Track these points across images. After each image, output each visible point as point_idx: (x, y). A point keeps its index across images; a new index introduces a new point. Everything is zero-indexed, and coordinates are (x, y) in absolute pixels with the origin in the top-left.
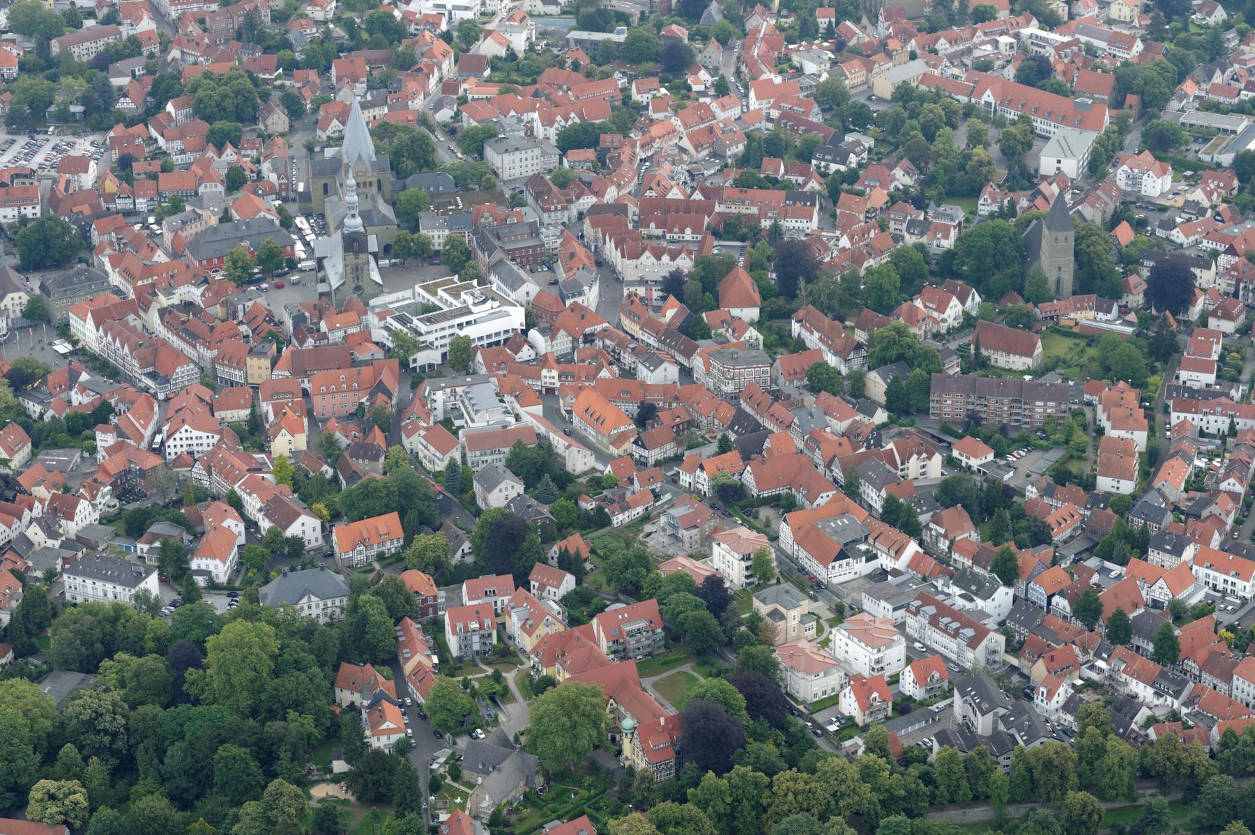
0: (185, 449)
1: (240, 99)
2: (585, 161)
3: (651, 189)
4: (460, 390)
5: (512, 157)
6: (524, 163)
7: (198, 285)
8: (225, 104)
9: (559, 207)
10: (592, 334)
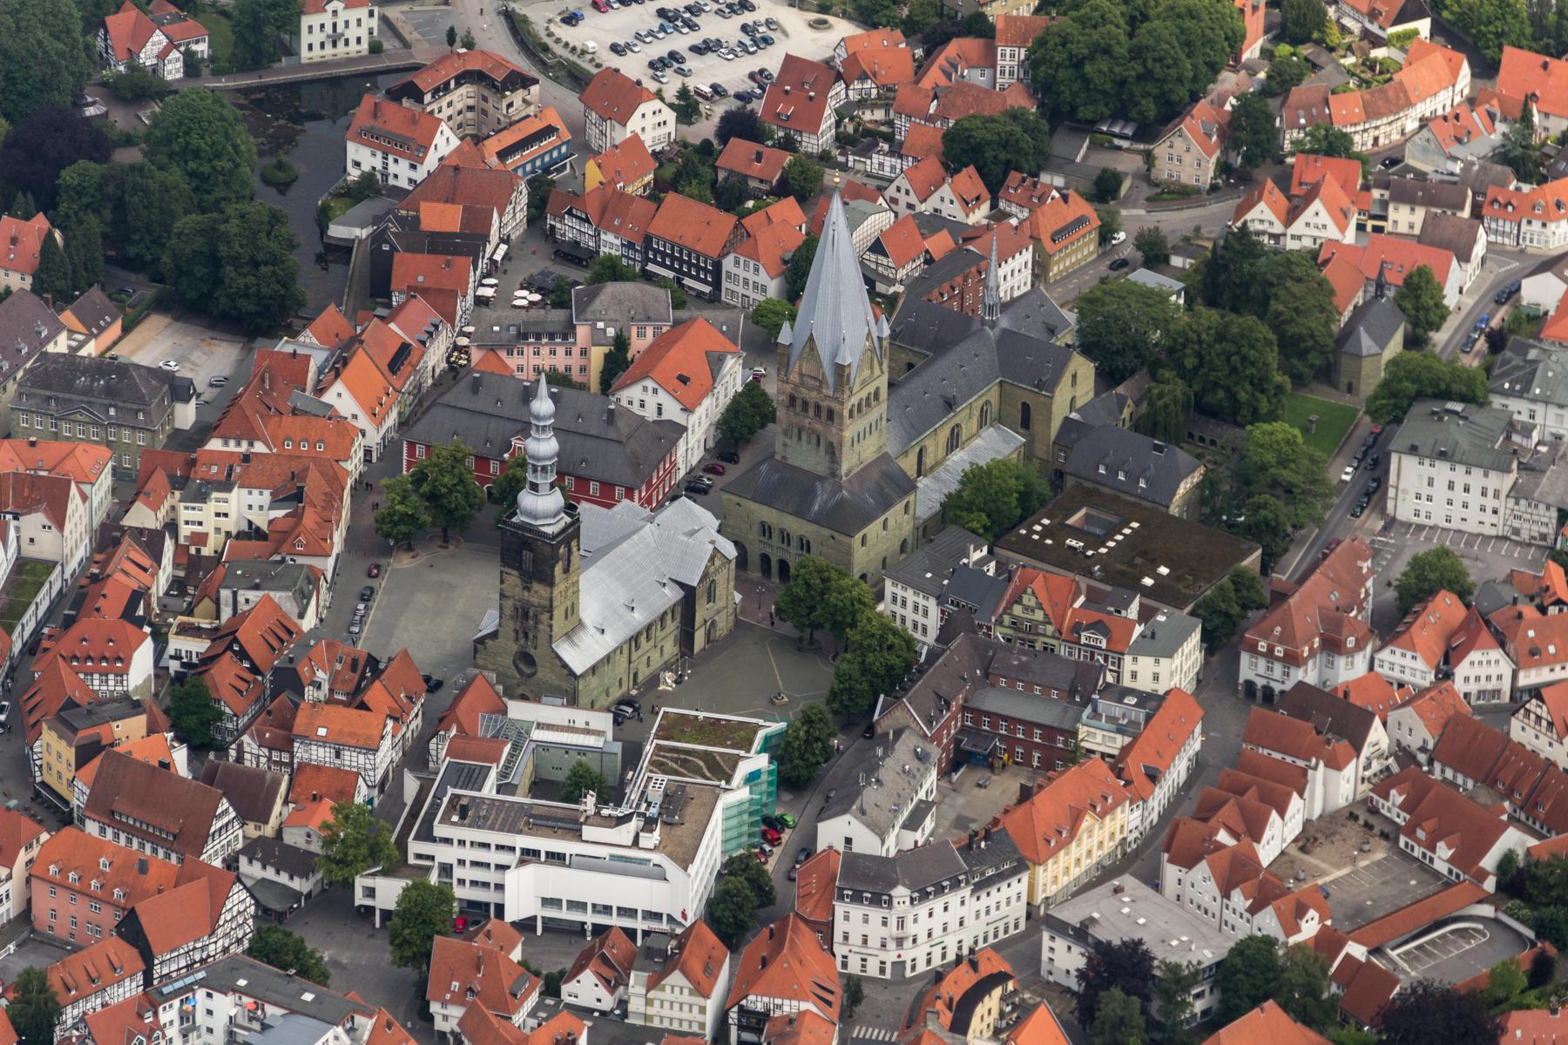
3: (1539, 697)
4: (270, 1009)
5: (1426, 470)
6: (1458, 495)
7: (276, 502)
9: (1279, 651)
10: (764, 1016)
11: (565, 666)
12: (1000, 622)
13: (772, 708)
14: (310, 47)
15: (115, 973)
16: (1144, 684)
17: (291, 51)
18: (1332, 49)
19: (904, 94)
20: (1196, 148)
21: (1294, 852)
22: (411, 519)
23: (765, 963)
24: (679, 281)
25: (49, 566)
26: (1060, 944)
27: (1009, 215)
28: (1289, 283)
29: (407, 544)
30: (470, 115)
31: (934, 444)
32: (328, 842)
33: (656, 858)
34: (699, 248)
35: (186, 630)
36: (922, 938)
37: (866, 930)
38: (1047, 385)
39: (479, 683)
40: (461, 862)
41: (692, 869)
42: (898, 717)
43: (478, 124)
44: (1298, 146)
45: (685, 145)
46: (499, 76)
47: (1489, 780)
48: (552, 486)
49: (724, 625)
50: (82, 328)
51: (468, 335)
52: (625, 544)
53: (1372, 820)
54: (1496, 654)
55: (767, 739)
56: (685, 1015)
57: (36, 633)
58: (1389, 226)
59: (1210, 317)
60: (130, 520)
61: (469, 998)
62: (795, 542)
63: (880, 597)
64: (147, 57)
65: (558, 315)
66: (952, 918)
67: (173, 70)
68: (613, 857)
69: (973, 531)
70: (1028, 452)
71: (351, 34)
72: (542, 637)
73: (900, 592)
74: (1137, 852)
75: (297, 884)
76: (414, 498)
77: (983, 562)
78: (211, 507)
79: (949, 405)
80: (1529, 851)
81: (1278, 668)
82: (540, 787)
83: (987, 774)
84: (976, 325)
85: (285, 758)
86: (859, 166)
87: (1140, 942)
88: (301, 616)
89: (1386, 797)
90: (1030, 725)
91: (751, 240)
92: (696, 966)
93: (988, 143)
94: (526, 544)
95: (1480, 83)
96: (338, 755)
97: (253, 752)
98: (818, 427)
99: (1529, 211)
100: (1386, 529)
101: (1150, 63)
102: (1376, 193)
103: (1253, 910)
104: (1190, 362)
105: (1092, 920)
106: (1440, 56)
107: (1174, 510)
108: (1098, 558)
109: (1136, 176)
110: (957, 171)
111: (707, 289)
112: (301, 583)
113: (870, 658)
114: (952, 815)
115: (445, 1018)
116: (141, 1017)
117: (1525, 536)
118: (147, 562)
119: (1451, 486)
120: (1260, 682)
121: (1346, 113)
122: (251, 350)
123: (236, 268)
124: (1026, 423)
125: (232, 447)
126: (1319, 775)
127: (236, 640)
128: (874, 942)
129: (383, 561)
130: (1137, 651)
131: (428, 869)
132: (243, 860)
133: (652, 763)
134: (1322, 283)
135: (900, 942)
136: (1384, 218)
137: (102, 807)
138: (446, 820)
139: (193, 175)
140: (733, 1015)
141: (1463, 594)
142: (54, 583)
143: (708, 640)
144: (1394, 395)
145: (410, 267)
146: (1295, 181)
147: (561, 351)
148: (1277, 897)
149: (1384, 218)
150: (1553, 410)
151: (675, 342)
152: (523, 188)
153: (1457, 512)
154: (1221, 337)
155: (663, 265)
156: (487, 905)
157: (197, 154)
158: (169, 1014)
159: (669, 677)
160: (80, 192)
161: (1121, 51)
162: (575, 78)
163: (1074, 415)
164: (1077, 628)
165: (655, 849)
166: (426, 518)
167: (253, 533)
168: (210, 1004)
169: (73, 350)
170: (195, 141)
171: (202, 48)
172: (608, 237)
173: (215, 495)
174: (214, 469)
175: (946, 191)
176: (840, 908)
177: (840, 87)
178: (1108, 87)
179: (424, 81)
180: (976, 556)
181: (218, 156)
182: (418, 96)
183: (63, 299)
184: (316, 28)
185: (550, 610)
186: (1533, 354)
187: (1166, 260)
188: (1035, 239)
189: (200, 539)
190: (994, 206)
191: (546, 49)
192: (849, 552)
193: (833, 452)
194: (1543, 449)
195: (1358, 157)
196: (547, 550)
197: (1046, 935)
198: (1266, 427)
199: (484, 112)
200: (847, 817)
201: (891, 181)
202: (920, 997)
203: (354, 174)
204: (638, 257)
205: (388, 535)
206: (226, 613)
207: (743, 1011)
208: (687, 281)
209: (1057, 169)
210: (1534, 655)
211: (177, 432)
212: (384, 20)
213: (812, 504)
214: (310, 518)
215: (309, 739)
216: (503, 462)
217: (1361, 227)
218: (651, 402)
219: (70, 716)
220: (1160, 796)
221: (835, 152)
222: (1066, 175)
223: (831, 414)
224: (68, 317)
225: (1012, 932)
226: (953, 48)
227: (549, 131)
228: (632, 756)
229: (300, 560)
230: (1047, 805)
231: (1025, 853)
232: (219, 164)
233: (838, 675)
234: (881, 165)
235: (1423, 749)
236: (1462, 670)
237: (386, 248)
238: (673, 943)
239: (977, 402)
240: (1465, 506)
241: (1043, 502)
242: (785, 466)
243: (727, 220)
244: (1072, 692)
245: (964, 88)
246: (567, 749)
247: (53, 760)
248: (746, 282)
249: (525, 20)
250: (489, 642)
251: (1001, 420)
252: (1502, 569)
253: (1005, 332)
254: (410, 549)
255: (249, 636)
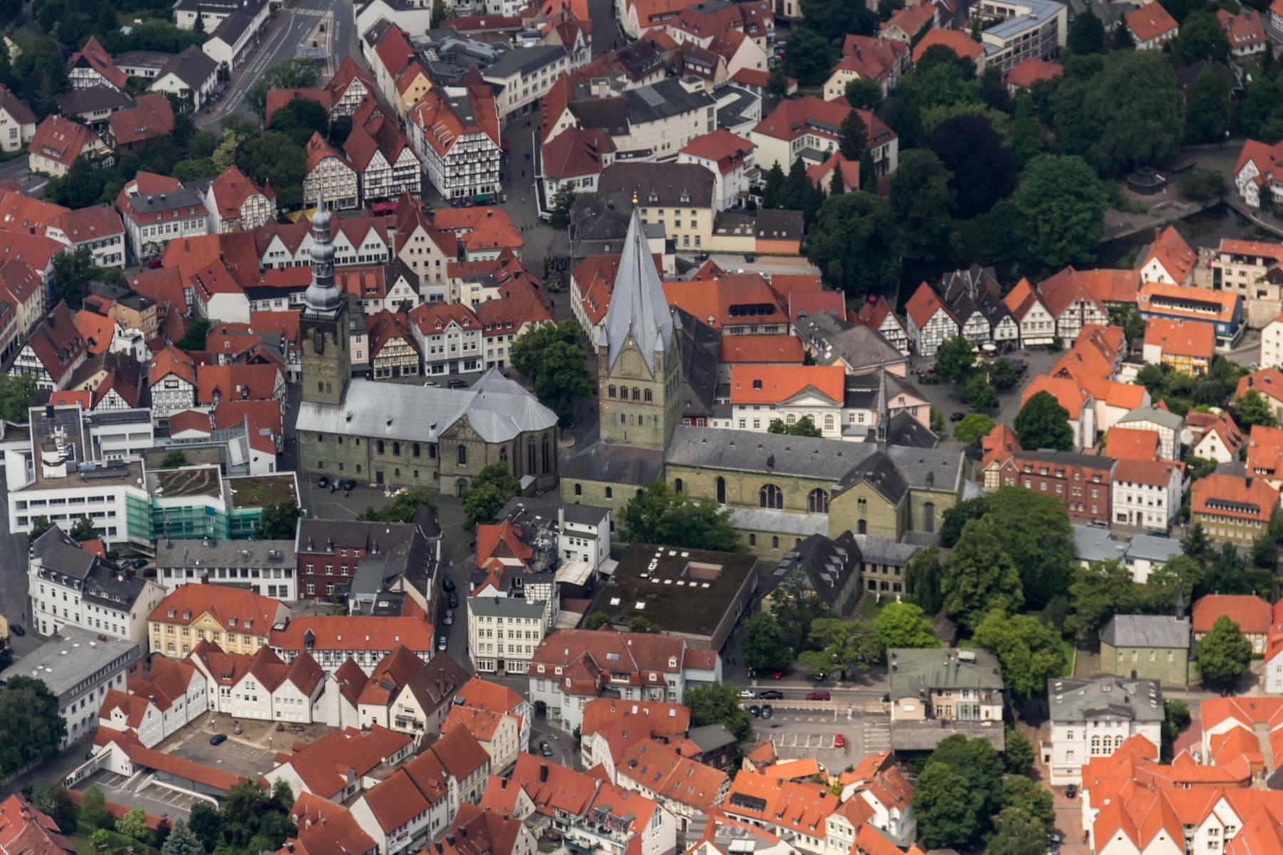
227: (1217, 307)
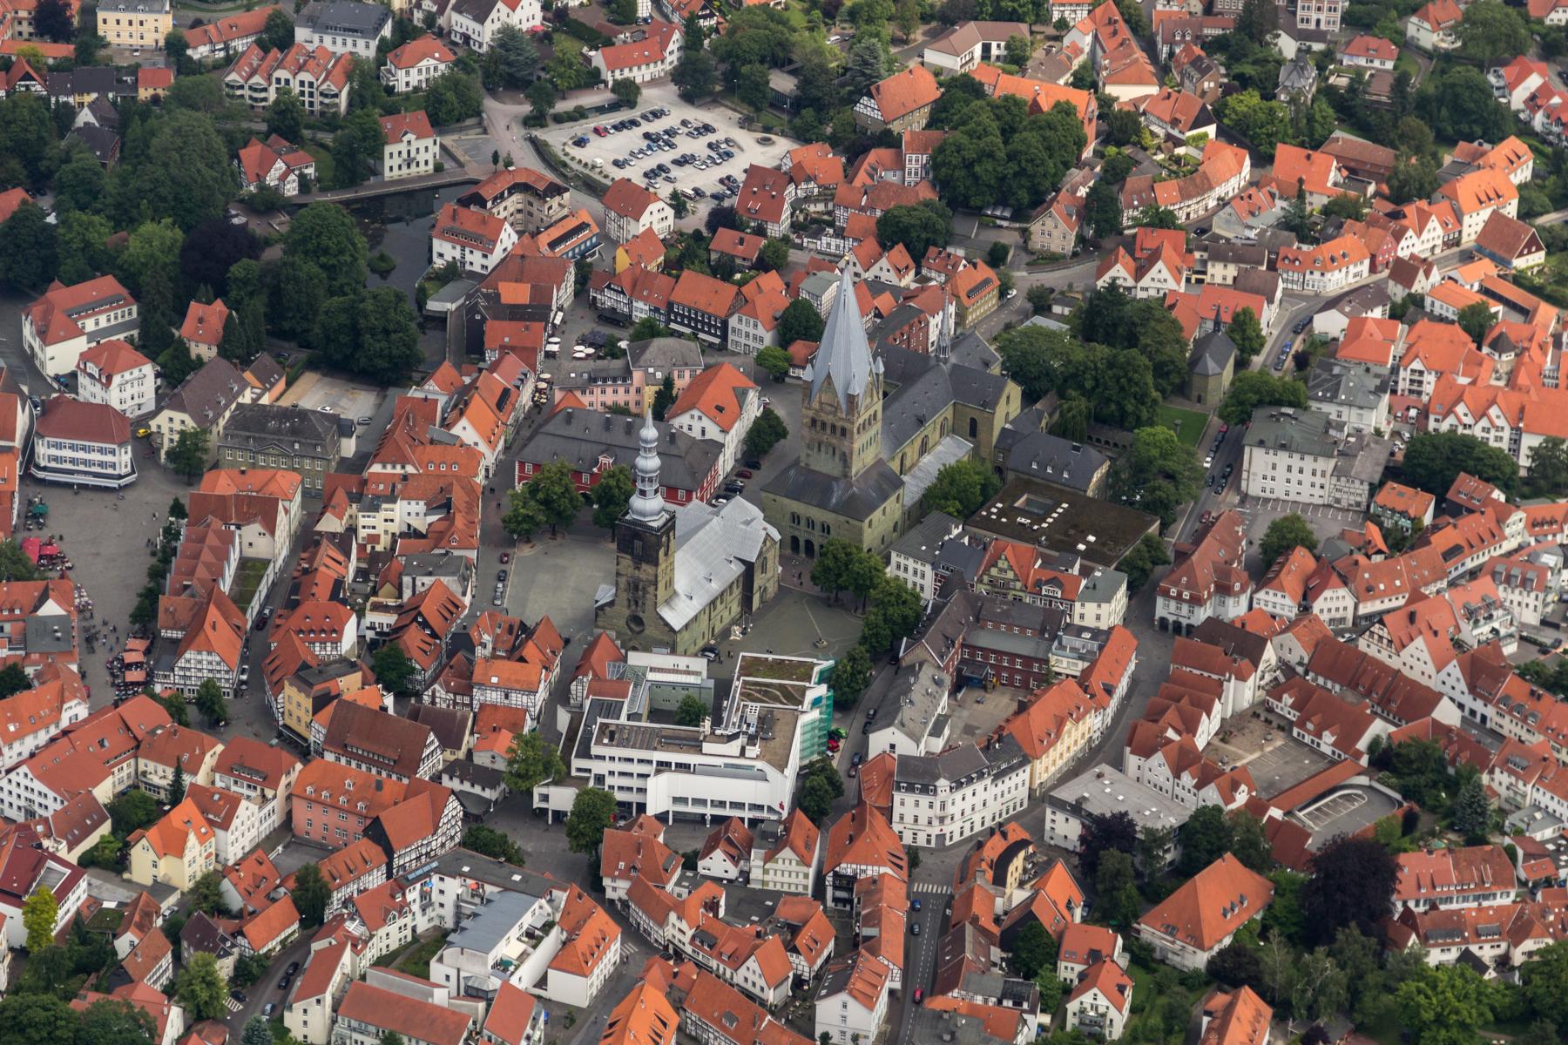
0: (22, 803)
1: (1013, 167)
2: (1403, 514)
3: (1381, 622)
4: (489, 889)
5: (1271, 458)
6: (1295, 476)
7: (431, 509)
8: (977, 169)
9: (1186, 595)
11: (667, 624)
12: (980, 581)
13: (816, 649)
14: (391, 169)
15: (366, 865)
16: (1090, 622)
17: (377, 172)
18: (1145, 149)
19: (842, 191)
20: (1062, 225)
21: (1217, 742)
22: (528, 518)
23: (851, 839)
24: (695, 335)
25: (265, 563)
26: (1060, 817)
27: (930, 279)
28: (1153, 323)
29: (527, 538)
30: (519, 216)
31: (911, 450)
32: (511, 763)
33: (759, 764)
34: (710, 310)
35: (378, 607)
36: (958, 816)
37: (917, 812)
38: (989, 404)
39: (603, 640)
40: (611, 773)
41: (787, 772)
42: (918, 653)
43: (525, 223)
44: (1137, 223)
45: (682, 234)
46: (541, 187)
47: (1352, 684)
48: (656, 491)
49: (772, 589)
50: (257, 384)
51: (544, 380)
52: (701, 533)
53: (1270, 717)
54: (1343, 592)
55: (821, 673)
56: (793, 880)
57: (260, 612)
58: (1208, 279)
59: (1102, 351)
60: (321, 527)
61: (633, 874)
62: (818, 527)
63: (888, 563)
64: (271, 179)
65: (617, 364)
66: (978, 800)
67: (291, 189)
68: (726, 765)
69: (950, 514)
70: (976, 452)
71: (421, 158)
72: (649, 603)
73: (902, 561)
74: (1100, 747)
75: (489, 794)
76: (532, 503)
77: (960, 536)
78: (382, 515)
79: (921, 422)
80: (1390, 736)
81: (1185, 608)
82: (655, 714)
83: (982, 693)
84: (933, 362)
85: (467, 700)
86: (812, 246)
87: (1126, 814)
88: (464, 594)
89: (1280, 700)
90: (1013, 656)
91: (750, 305)
92: (800, 843)
93: (913, 226)
94: (636, 535)
95: (1259, 172)
96: (507, 697)
97: (440, 696)
98: (834, 441)
99: (1312, 264)
100: (1243, 502)
101: (1023, 164)
102: (1197, 255)
103: (1199, 786)
104: (1089, 384)
105: (1084, 798)
106: (1229, 152)
107: (1090, 493)
108: (1042, 531)
109: (1017, 247)
110: (892, 247)
111: (717, 341)
112: (462, 570)
113: (891, 610)
114: (961, 725)
115: (614, 889)
116: (393, 897)
117: (1344, 504)
118: (341, 558)
119: (1289, 469)
120: (1171, 618)
121: (1167, 196)
122: (385, 397)
123: (373, 335)
124: (973, 432)
125: (389, 469)
126: (1231, 686)
127: (420, 614)
128: (923, 820)
129: (509, 551)
130: (1084, 599)
131: (587, 779)
132: (445, 778)
133: (742, 694)
134: (1174, 322)
135: (942, 820)
136: (1204, 273)
137: (337, 740)
138: (599, 742)
139: (323, 266)
140: (829, 879)
141: (1311, 547)
142: (270, 575)
143: (762, 601)
144: (1241, 403)
145: (498, 332)
146: (1138, 247)
147: (621, 390)
148: (1217, 776)
149: (1204, 273)
150: (1355, 411)
151: (710, 382)
152: (572, 270)
153: (1294, 487)
154: (1111, 365)
155: (682, 324)
156: (630, 804)
157: (326, 251)
158: (413, 895)
159: (737, 629)
160: (245, 282)
161: (1001, 155)
162: (592, 187)
163: (1008, 426)
164: (1039, 584)
165: (757, 758)
166: (541, 518)
167: (412, 533)
168: (442, 886)
169: (254, 401)
170: (325, 241)
171: (310, 171)
172: (639, 305)
173: (384, 506)
174: (381, 487)
175: (884, 262)
176: (897, 797)
177: (791, 188)
178: (993, 182)
179: (487, 193)
180: (956, 532)
181: (341, 252)
182: (482, 203)
183: (245, 362)
184: (396, 155)
185: (655, 583)
186: (1336, 370)
187: (1049, 308)
188: (957, 296)
189: (374, 539)
190: (917, 273)
191: (565, 165)
192: (860, 532)
193: (846, 460)
194: (1352, 440)
195: (1180, 228)
196: (653, 539)
197: (1049, 811)
198: (1149, 430)
199: (531, 214)
200: (892, 729)
201: (842, 257)
202: (966, 860)
203: (439, 263)
204: (663, 318)
205: (514, 531)
206: (407, 594)
207: (836, 875)
208: (701, 335)
209: (959, 244)
210: (1369, 591)
211: (343, 460)
212: (443, 147)
213: (829, 499)
214: (459, 521)
215: (484, 685)
216: (592, 474)
217: (1188, 280)
218: (697, 426)
219: (305, 675)
220: (1114, 703)
221: (793, 236)
222: (966, 248)
223: (844, 432)
224: (248, 375)
225: (1019, 809)
226: (874, 156)
228: (723, 689)
229: (456, 553)
230: (1039, 714)
231: (1028, 751)
232: (342, 258)
233: (867, 625)
234: (829, 245)
235: (1300, 664)
236: (1318, 606)
237: (478, 317)
238: (781, 827)
239: (938, 418)
240: (1300, 483)
241: (996, 492)
242: (809, 471)
243: (729, 290)
244: (1042, 631)
245: (884, 185)
246: (674, 686)
247: (293, 708)
248: (747, 335)
249: (546, 144)
250: (607, 609)
251: (954, 431)
252: (1335, 530)
253: (954, 366)
254: (528, 541)
255: (429, 609)
